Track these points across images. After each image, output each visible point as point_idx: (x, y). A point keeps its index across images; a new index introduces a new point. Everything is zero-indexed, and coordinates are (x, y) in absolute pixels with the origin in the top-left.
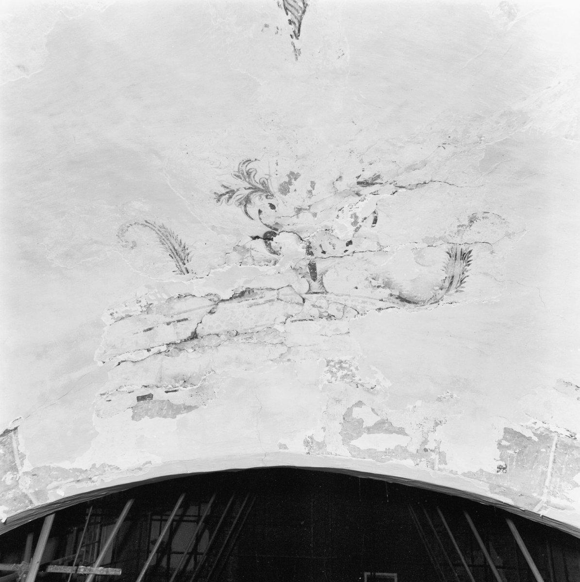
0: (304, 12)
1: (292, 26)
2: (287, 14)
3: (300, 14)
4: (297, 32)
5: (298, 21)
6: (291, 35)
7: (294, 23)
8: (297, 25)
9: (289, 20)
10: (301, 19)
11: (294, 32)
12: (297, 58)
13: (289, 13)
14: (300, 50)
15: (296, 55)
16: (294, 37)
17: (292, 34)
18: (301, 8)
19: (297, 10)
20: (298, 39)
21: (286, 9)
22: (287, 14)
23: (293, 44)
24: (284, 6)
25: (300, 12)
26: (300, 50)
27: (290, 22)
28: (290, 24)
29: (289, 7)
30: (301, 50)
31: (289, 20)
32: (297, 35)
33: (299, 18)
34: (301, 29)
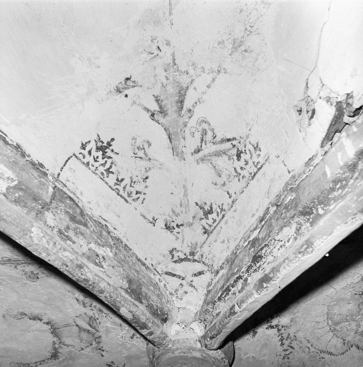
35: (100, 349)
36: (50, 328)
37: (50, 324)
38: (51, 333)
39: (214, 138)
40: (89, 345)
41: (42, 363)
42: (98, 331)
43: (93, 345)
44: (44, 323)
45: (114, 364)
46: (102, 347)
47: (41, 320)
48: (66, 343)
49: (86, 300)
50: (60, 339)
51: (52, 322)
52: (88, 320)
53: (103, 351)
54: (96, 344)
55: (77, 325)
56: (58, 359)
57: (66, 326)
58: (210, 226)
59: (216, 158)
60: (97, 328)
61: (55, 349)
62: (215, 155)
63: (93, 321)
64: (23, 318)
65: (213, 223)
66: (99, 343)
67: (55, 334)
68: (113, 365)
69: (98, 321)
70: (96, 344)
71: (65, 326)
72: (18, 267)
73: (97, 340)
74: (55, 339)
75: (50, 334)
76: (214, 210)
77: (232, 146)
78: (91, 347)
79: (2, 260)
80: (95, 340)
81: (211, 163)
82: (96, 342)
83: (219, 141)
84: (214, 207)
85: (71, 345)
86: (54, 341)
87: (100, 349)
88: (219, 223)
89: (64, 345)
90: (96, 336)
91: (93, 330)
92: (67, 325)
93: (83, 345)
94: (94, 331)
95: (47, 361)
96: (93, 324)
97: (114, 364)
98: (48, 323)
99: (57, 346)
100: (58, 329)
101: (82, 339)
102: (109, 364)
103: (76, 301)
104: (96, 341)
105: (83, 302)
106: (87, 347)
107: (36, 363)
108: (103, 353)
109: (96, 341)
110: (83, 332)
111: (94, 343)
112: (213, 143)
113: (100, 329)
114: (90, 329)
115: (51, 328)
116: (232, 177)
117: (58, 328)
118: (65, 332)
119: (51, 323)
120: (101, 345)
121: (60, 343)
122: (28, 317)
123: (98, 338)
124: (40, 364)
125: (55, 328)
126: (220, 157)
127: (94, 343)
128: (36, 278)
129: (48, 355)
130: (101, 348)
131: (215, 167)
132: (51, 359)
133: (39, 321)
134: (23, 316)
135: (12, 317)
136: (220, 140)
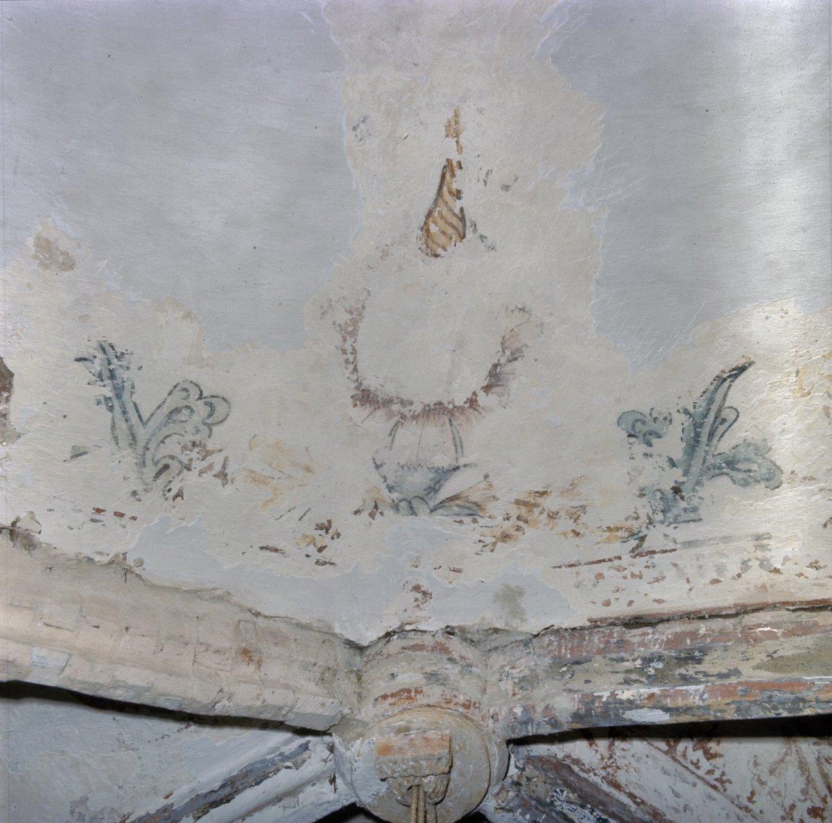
0: (430, 214)
1: (454, 187)
2: (462, 209)
3: (437, 209)
4: (448, 176)
5: (442, 197)
6: (461, 168)
7: (450, 192)
8: (445, 189)
9: (459, 198)
10: (436, 200)
11: (453, 175)
12: (456, 115)
13: (457, 211)
14: (447, 136)
15: (457, 123)
16: (455, 164)
17: (458, 172)
18: (433, 222)
19: (442, 217)
20: (448, 160)
21: (462, 219)
22: (462, 209)
23: (460, 149)
24: (464, 226)
25: (436, 214)
26: (447, 136)
27: (458, 195)
28: (459, 192)
29: (455, 221)
30: (444, 134)
31: (459, 198)
32: (449, 169)
33: (440, 201)
34: (439, 180)
35: (376, 507)
36: (457, 404)
37: (470, 407)
38: (441, 403)
39: (827, 760)
40: (390, 482)
41: (351, 367)
42: (432, 511)
43: (390, 492)
44: (474, 394)
45: (333, 538)
46: (382, 513)
47: (487, 389)
48: (401, 431)
49: (541, 513)
50: (414, 417)
51: (476, 413)
52: (473, 499)
53: (372, 515)
54: (393, 500)
55: (457, 468)
56: (355, 405)
57: (458, 444)
58: (684, 756)
59: (796, 763)
60: (441, 511)
61: (388, 402)
62: (800, 762)
63: (468, 508)
64: (503, 351)
65: (692, 763)
66: (396, 507)
67: (435, 409)
68: (329, 536)
69: (467, 520)
70: (393, 500)
71: (457, 439)
72: (684, 418)
73: (403, 504)
74: (418, 408)
75: (435, 400)
76: (713, 761)
77: (823, 796)
78: (383, 487)
79: (727, 404)
80: (404, 500)
81: (786, 754)
82: (397, 502)
83: (823, 770)
84: (718, 762)
85: (393, 440)
86: (411, 403)
87: (376, 507)
88: (694, 773)
89: (396, 425)
90: (415, 503)
91: (437, 502)
92: (458, 445)
93: (388, 470)
94: (432, 504)
95: (354, 377)
96: (458, 506)
97: (333, 538)
98: (473, 402)
99: (395, 407)
100: (450, 420)
101: (409, 469)
102: (333, 525)
103: (541, 490)
104: (401, 501)
105: (536, 505)
106: (385, 477)
107: (354, 352)
108: (365, 515)
109: (401, 501)
110: (431, 475)
111: (395, 495)
112: (819, 757)
113: (438, 517)
114: (445, 493)
115: (455, 407)
116: (780, 800)
117: (454, 423)
118: (433, 432)
119: (471, 411)
120: (389, 513)
121: (403, 417)
122: (503, 361)
123: (411, 508)
124: (347, 361)
125: (452, 415)
126: (799, 771)
127: (395, 495)
128: (633, 433)
129: (371, 383)
130: (379, 511)
131: (782, 761)
132: (357, 388)
133: (485, 384)
134: (508, 353)
135: (516, 330)
136: (826, 771)
